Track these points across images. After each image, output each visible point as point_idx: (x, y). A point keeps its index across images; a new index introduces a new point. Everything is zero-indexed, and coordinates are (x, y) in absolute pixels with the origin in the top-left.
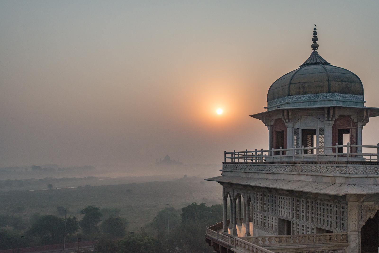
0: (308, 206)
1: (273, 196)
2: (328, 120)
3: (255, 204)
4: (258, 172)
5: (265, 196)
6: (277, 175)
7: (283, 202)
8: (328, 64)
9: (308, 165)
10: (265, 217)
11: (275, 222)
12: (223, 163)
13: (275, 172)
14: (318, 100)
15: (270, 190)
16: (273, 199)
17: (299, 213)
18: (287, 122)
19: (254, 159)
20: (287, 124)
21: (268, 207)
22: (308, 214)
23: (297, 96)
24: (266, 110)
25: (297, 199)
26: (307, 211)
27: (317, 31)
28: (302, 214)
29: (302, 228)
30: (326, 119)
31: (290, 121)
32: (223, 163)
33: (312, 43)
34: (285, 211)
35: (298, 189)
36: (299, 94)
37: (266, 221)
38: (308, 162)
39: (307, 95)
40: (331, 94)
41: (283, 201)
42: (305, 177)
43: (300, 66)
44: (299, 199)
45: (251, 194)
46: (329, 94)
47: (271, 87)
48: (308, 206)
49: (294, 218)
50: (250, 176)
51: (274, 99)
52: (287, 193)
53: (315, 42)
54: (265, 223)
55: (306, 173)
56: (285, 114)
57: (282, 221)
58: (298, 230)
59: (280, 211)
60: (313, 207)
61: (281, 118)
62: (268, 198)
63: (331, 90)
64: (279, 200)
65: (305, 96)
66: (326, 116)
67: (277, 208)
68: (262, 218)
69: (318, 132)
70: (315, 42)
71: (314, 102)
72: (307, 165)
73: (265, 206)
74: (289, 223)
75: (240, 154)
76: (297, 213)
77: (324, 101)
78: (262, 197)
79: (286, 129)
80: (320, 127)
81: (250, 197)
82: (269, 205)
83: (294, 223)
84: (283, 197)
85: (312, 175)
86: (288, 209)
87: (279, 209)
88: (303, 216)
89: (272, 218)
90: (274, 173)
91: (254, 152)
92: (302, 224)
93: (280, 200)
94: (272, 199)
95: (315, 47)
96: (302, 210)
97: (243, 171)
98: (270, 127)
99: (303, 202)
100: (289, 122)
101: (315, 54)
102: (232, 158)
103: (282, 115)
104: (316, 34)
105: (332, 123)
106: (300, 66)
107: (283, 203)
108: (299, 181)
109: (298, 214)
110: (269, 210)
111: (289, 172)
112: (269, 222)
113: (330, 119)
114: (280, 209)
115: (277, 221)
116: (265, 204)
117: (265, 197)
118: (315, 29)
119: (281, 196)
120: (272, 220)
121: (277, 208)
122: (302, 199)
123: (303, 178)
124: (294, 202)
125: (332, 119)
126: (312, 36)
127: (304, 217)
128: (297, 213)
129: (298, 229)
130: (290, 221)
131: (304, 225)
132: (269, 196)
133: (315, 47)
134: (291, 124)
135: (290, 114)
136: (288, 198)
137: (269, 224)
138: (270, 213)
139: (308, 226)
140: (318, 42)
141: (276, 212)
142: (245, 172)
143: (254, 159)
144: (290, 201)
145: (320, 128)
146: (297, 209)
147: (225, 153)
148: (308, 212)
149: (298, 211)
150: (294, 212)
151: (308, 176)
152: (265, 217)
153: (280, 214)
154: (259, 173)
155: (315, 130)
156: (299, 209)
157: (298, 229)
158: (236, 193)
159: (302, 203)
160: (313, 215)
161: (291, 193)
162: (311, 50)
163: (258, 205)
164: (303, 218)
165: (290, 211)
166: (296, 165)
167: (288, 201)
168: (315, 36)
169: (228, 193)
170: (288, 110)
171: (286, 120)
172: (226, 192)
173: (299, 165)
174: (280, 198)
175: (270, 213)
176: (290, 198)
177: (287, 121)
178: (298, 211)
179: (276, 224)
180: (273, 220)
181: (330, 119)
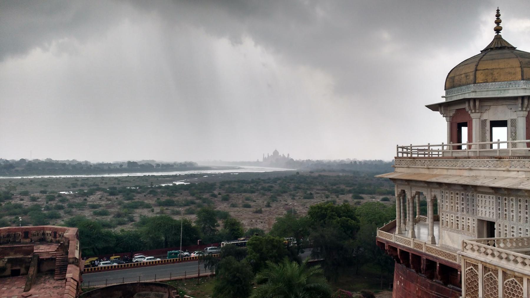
0: (520, 205)
1: (469, 195)
2: (522, 110)
3: (443, 203)
4: (447, 167)
5: (457, 194)
6: (475, 171)
7: (484, 202)
8: (514, 48)
9: (520, 160)
10: (457, 217)
11: (473, 224)
12: (396, 158)
13: (472, 168)
14: (510, 88)
15: (465, 187)
16: (469, 197)
17: (507, 213)
18: (472, 113)
19: (427, 154)
20: (472, 115)
21: (462, 206)
22: (519, 215)
23: (484, 84)
24: (444, 100)
25: (504, 197)
26: (519, 210)
27: (500, 12)
28: (512, 214)
29: (512, 230)
30: (520, 109)
31: (477, 111)
32: (396, 158)
33: (495, 25)
34: (487, 209)
35: (515, 187)
36: (487, 82)
37: (459, 223)
38: (519, 157)
39: (497, 83)
40: (524, 81)
41: (484, 199)
42: (515, 173)
43: (481, 51)
44: (507, 198)
45: (437, 193)
46: (522, 81)
47: (449, 74)
48: (520, 205)
49: (499, 218)
50: (434, 173)
51: (453, 87)
52: (491, 191)
53: (498, 25)
54: (458, 224)
55: (517, 169)
56: (472, 103)
57: (481, 222)
58: (505, 232)
59: (480, 211)
60: (527, 206)
61: (464, 109)
62: (462, 197)
63: (525, 78)
64: (478, 199)
65: (494, 83)
66: (520, 105)
67: (474, 208)
68: (453, 218)
69: (509, 123)
70: (498, 25)
71: (505, 90)
72: (518, 160)
73: (457, 206)
74: (493, 223)
75: (413, 148)
76: (505, 213)
77: (517, 89)
78: (453, 195)
79: (472, 121)
80: (512, 118)
81: (435, 197)
82: (463, 204)
83: (500, 225)
84: (483, 195)
85: (525, 172)
86: (491, 208)
87: (478, 209)
88: (513, 216)
89: (469, 219)
90: (470, 169)
91: (440, 145)
92: (512, 226)
93: (480, 199)
94: (468, 197)
95: (498, 30)
96: (511, 209)
97: (425, 167)
98: (448, 118)
99: (512, 200)
100: (475, 112)
101: (498, 38)
102: (403, 153)
103: (467, 105)
104: (500, 15)
105: (526, 113)
106: (481, 51)
107: (484, 202)
108: (507, 178)
109: (506, 215)
110: (463, 210)
111: (492, 168)
112: (464, 223)
113: (524, 109)
114: (480, 209)
115: (476, 222)
116: (457, 203)
117: (457, 196)
118: (498, 11)
119: (480, 195)
120: (468, 221)
121: (474, 208)
122: (511, 198)
123: (513, 174)
124: (500, 201)
125: (526, 108)
126: (495, 18)
127: (515, 217)
128: (505, 213)
129: (506, 230)
130: (494, 223)
131: (515, 226)
132: (463, 195)
133: (498, 30)
134: (479, 115)
135: (477, 103)
136: (491, 196)
137: (463, 225)
138: (465, 213)
139: (519, 227)
140: (501, 25)
141: (474, 212)
142: (429, 168)
143: (427, 154)
144: (494, 200)
145: (512, 120)
146: (505, 208)
147: (398, 147)
148: (520, 212)
149: (506, 210)
150: (500, 212)
151: (520, 172)
152: (457, 217)
153: (480, 215)
154: (448, 169)
155: (506, 121)
156: (507, 209)
157: (506, 230)
158: (414, 192)
159: (511, 202)
160: (527, 216)
161: (496, 191)
162: (494, 34)
163: (448, 204)
164: (513, 218)
165: (494, 211)
166: (502, 160)
167: (491, 200)
168: (498, 19)
169: (403, 192)
170: (475, 100)
171: (472, 110)
172: (400, 190)
173: (507, 160)
174: (480, 196)
175: (465, 213)
176: (494, 196)
177: (473, 111)
178: (506, 210)
179: (474, 225)
180: (469, 221)
181: (524, 109)
